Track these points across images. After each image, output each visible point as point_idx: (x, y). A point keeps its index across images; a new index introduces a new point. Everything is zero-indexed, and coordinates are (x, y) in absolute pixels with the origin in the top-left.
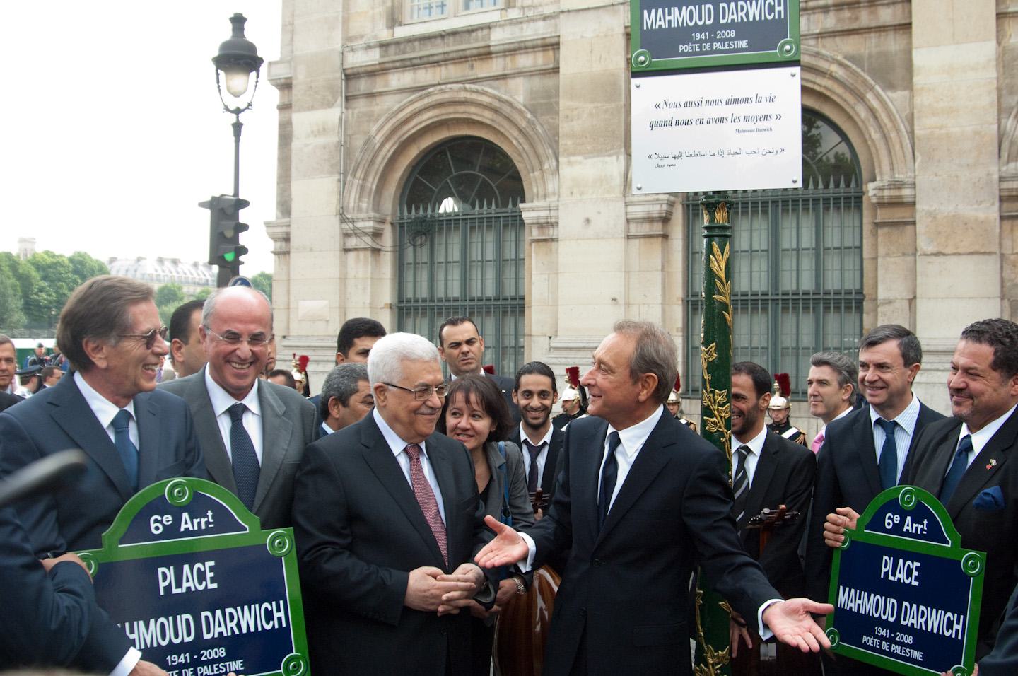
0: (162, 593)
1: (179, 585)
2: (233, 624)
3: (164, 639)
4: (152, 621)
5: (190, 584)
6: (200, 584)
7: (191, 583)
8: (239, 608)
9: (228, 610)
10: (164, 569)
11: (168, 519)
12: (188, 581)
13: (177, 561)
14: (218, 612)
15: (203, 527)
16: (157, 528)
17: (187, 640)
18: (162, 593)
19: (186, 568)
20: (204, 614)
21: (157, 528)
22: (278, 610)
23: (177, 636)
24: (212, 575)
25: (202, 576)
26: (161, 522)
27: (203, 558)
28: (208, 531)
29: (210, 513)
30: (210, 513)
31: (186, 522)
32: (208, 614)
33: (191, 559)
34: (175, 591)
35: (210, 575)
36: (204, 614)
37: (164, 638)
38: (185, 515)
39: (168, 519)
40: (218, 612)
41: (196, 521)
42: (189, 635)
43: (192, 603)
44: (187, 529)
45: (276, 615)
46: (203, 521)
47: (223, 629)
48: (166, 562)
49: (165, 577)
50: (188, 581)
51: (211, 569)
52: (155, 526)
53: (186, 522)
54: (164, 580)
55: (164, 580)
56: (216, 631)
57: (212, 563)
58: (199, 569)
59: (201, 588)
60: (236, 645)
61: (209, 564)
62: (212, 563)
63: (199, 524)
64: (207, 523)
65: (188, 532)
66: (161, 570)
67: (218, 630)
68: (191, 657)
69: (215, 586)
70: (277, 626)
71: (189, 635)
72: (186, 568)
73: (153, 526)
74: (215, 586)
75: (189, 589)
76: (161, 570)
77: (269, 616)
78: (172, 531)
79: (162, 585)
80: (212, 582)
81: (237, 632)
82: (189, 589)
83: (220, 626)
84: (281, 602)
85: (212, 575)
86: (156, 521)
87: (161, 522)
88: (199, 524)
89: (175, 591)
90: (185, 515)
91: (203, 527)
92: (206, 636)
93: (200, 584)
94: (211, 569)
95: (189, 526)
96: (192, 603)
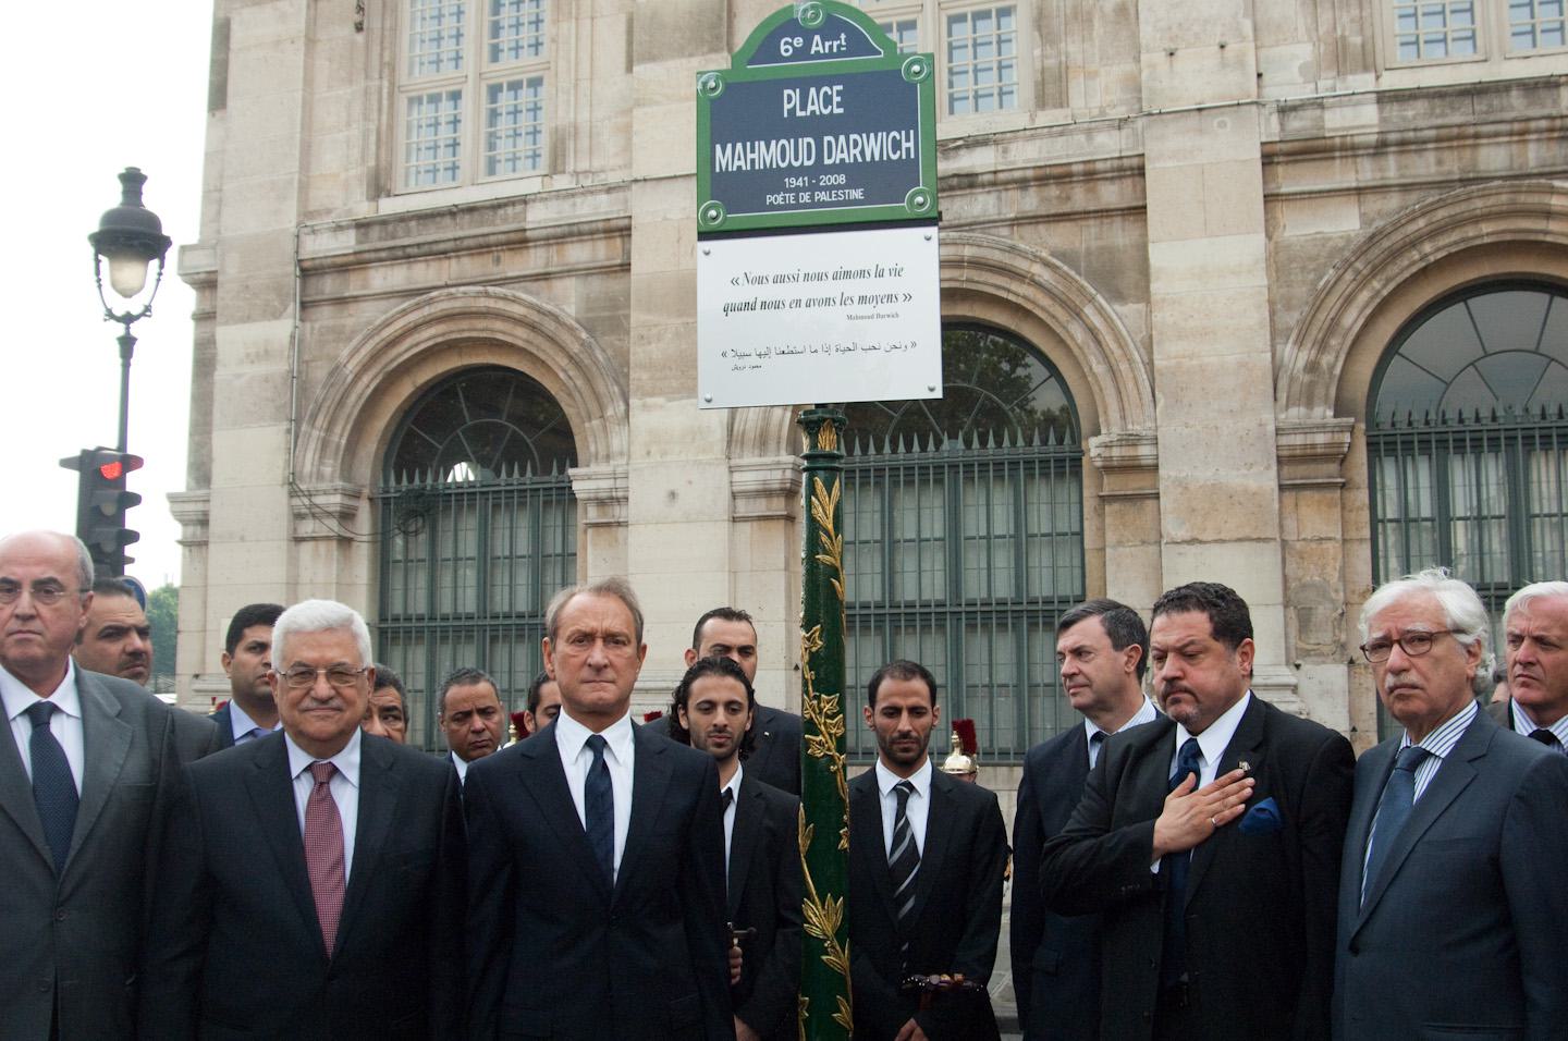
0: (786, 115)
1: (804, 108)
2: (857, 151)
3: (783, 160)
4: (773, 142)
5: (816, 108)
6: (826, 107)
7: (816, 106)
8: (864, 135)
9: (852, 137)
10: (790, 92)
11: (798, 42)
12: (813, 104)
13: (803, 84)
14: (842, 138)
15: (835, 50)
16: (787, 51)
17: (807, 163)
18: (786, 115)
19: (813, 91)
20: (826, 139)
21: (787, 51)
22: (908, 140)
23: (796, 159)
24: (839, 99)
25: (828, 100)
26: (792, 44)
27: (831, 81)
28: (840, 54)
29: (843, 36)
30: (843, 36)
31: (818, 45)
32: (831, 138)
33: (819, 81)
34: (799, 113)
35: (836, 99)
36: (826, 139)
37: (783, 160)
38: (817, 38)
39: (798, 42)
40: (842, 138)
41: (827, 44)
42: (809, 159)
43: (818, 127)
44: (817, 52)
45: (905, 145)
46: (836, 43)
47: (845, 155)
48: (792, 84)
49: (791, 99)
50: (813, 104)
51: (839, 93)
52: (785, 48)
53: (818, 45)
54: (789, 101)
55: (789, 101)
56: (837, 157)
57: (840, 88)
58: (826, 93)
59: (826, 112)
60: (857, 173)
61: (836, 88)
62: (840, 88)
63: (831, 47)
64: (839, 46)
65: (818, 55)
66: (786, 92)
67: (840, 156)
68: (809, 182)
69: (841, 111)
70: (904, 157)
71: (809, 159)
72: (813, 91)
73: (783, 48)
74: (841, 111)
75: (813, 112)
76: (786, 92)
77: (896, 145)
78: (802, 53)
79: (787, 107)
80: (838, 107)
81: (860, 160)
82: (813, 112)
83: (842, 152)
84: (912, 132)
85: (839, 99)
86: (786, 43)
87: (792, 44)
88: (831, 47)
89: (799, 113)
90: (817, 38)
91: (835, 50)
92: (827, 162)
93: (826, 107)
94: (839, 93)
95: (820, 49)
96: (818, 127)
